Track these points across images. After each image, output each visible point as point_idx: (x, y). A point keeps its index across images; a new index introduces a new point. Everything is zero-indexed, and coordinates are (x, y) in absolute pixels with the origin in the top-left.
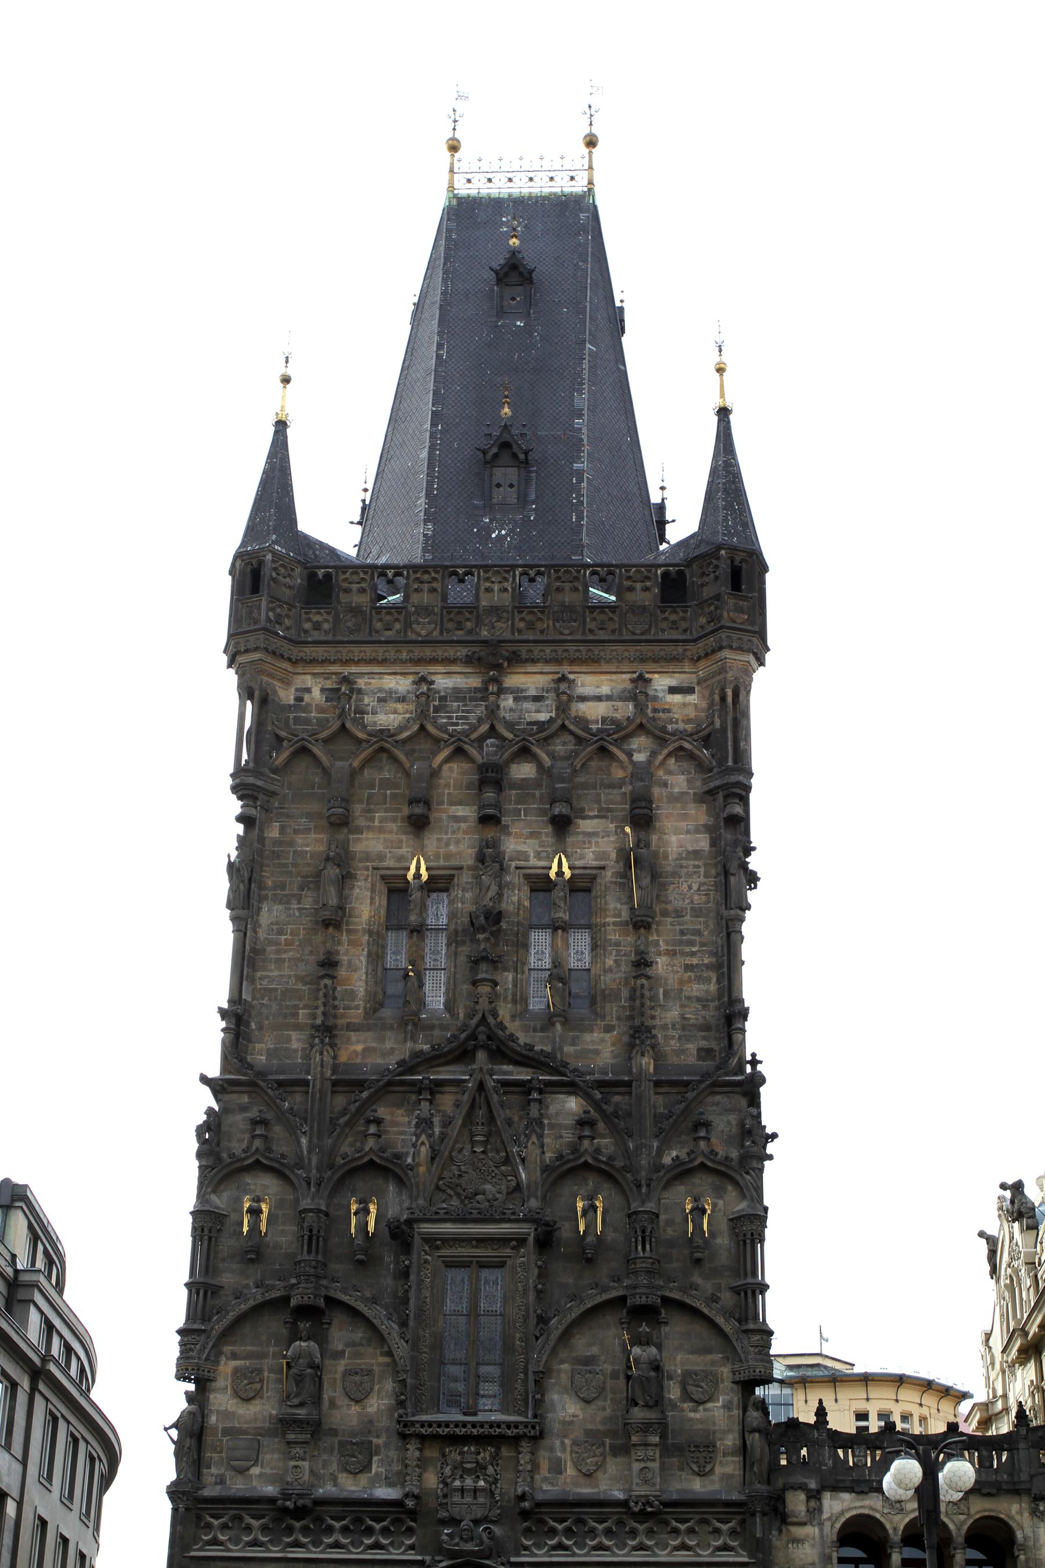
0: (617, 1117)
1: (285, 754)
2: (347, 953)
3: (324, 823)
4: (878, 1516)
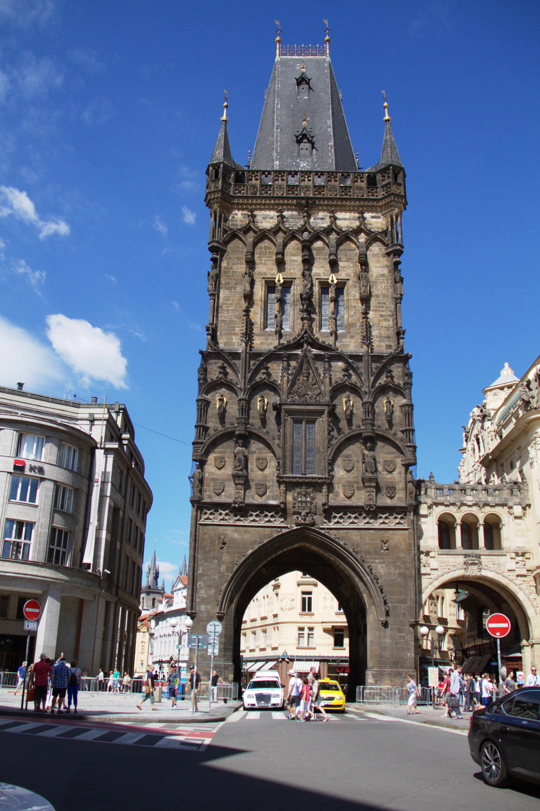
3: (244, 261)
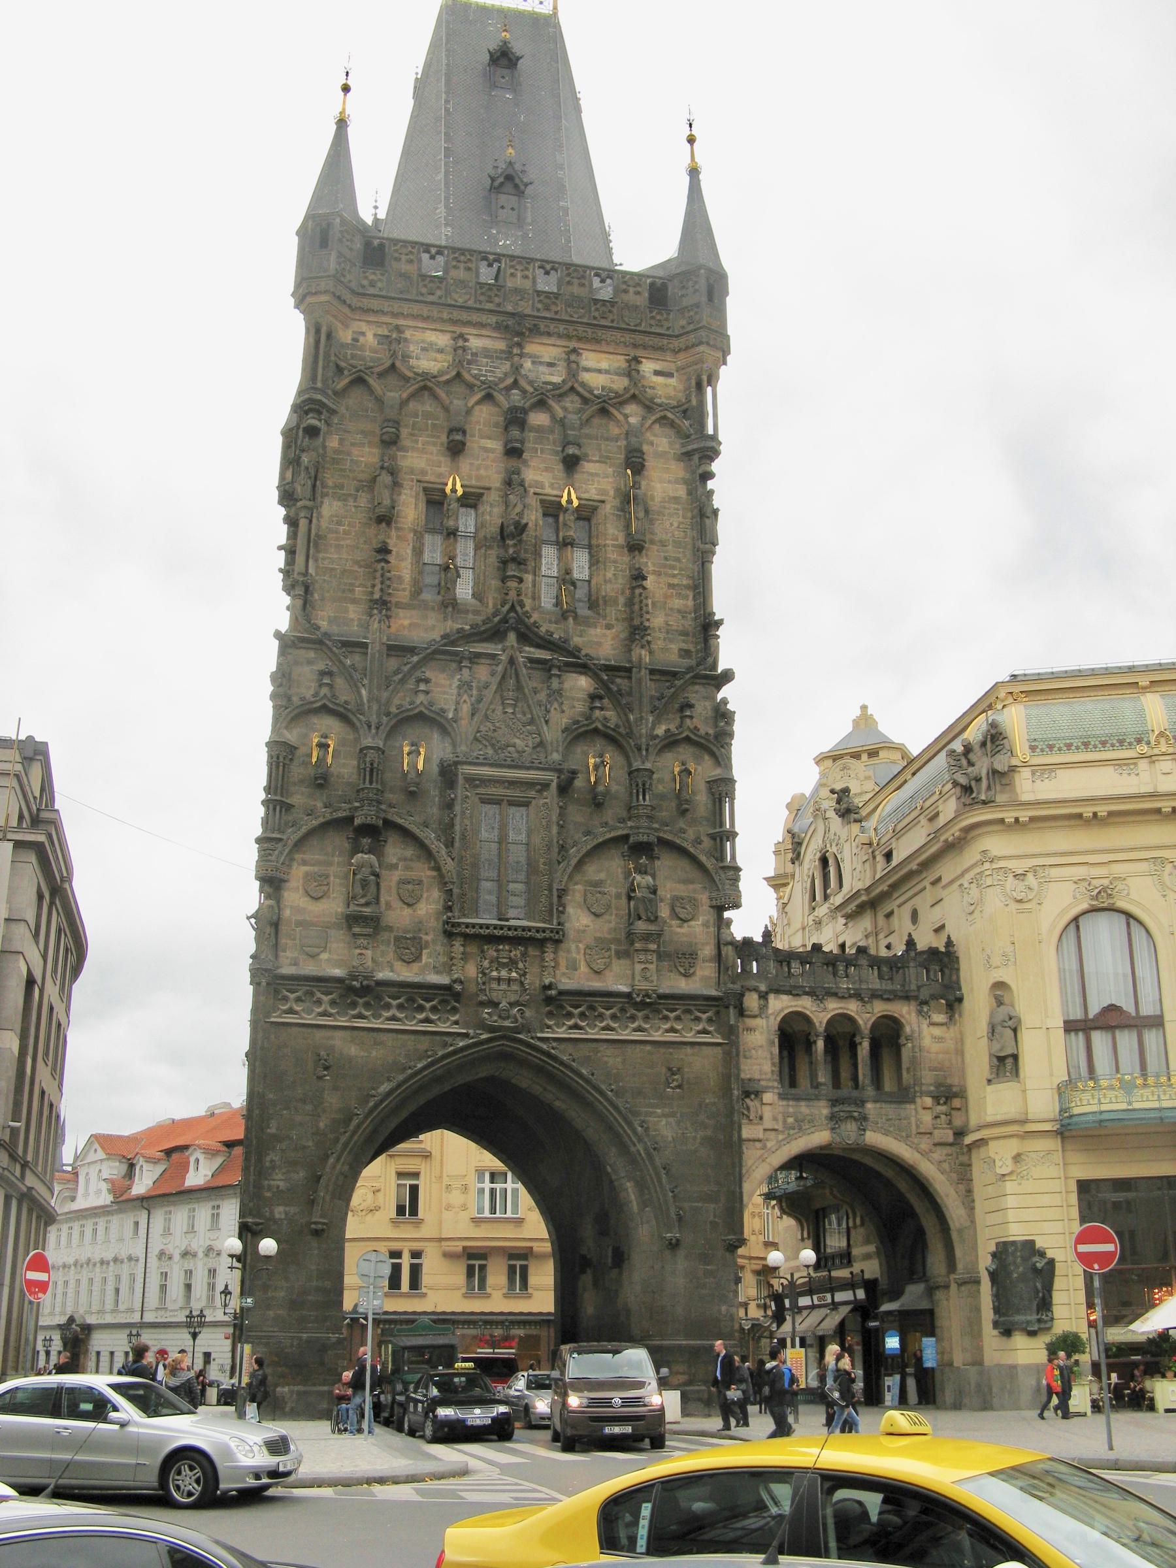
1: (347, 381)
2: (395, 545)
3: (377, 439)
4: (808, 1013)
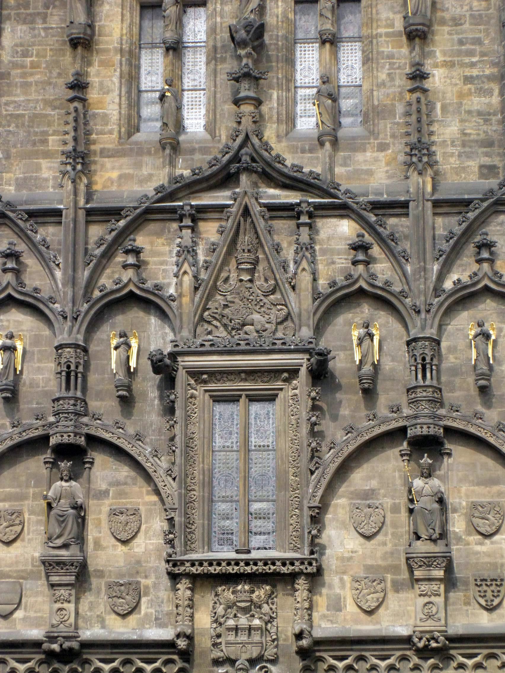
0: (393, 240)
2: (98, 74)
